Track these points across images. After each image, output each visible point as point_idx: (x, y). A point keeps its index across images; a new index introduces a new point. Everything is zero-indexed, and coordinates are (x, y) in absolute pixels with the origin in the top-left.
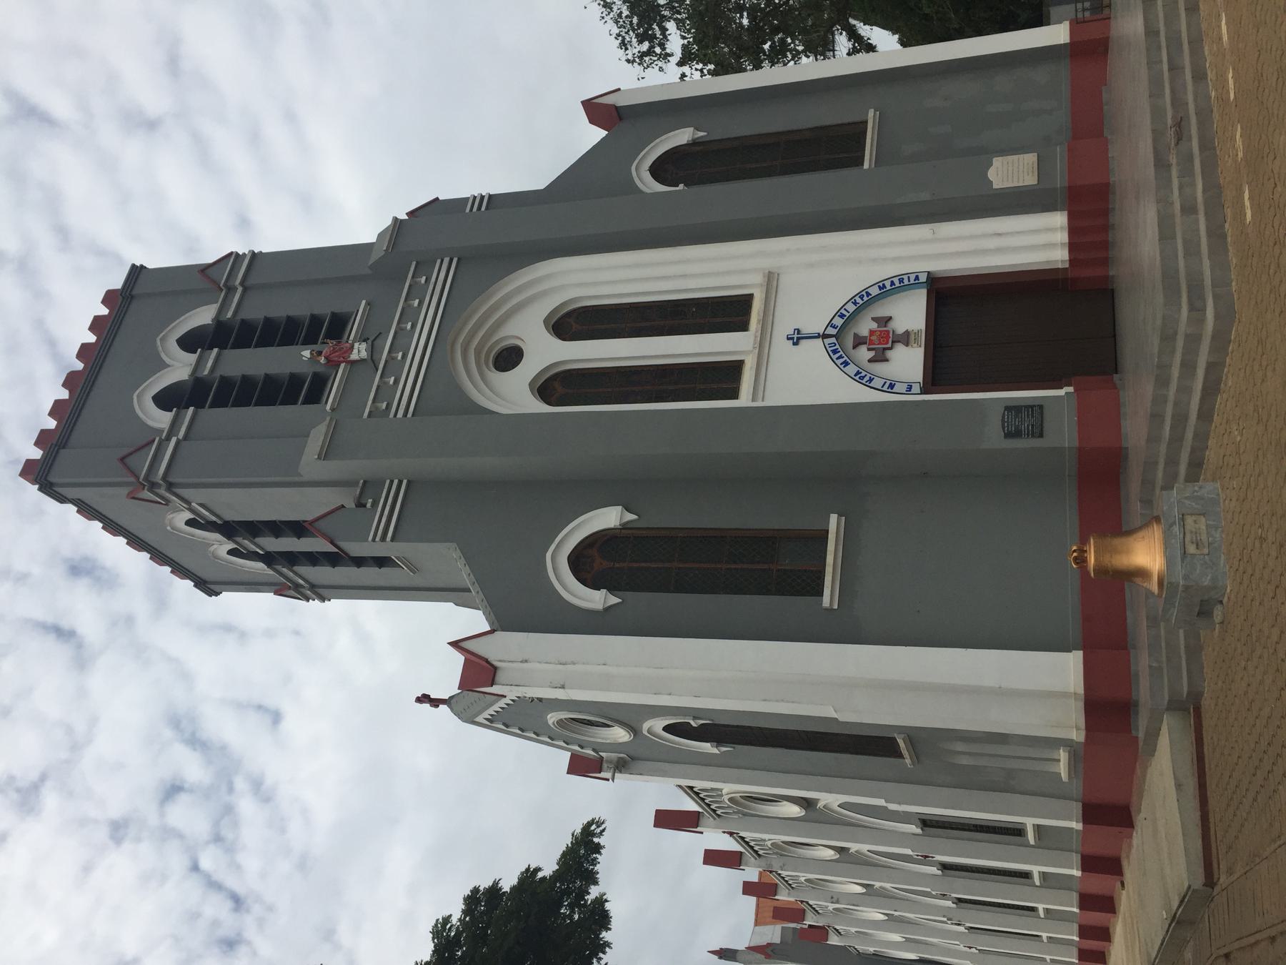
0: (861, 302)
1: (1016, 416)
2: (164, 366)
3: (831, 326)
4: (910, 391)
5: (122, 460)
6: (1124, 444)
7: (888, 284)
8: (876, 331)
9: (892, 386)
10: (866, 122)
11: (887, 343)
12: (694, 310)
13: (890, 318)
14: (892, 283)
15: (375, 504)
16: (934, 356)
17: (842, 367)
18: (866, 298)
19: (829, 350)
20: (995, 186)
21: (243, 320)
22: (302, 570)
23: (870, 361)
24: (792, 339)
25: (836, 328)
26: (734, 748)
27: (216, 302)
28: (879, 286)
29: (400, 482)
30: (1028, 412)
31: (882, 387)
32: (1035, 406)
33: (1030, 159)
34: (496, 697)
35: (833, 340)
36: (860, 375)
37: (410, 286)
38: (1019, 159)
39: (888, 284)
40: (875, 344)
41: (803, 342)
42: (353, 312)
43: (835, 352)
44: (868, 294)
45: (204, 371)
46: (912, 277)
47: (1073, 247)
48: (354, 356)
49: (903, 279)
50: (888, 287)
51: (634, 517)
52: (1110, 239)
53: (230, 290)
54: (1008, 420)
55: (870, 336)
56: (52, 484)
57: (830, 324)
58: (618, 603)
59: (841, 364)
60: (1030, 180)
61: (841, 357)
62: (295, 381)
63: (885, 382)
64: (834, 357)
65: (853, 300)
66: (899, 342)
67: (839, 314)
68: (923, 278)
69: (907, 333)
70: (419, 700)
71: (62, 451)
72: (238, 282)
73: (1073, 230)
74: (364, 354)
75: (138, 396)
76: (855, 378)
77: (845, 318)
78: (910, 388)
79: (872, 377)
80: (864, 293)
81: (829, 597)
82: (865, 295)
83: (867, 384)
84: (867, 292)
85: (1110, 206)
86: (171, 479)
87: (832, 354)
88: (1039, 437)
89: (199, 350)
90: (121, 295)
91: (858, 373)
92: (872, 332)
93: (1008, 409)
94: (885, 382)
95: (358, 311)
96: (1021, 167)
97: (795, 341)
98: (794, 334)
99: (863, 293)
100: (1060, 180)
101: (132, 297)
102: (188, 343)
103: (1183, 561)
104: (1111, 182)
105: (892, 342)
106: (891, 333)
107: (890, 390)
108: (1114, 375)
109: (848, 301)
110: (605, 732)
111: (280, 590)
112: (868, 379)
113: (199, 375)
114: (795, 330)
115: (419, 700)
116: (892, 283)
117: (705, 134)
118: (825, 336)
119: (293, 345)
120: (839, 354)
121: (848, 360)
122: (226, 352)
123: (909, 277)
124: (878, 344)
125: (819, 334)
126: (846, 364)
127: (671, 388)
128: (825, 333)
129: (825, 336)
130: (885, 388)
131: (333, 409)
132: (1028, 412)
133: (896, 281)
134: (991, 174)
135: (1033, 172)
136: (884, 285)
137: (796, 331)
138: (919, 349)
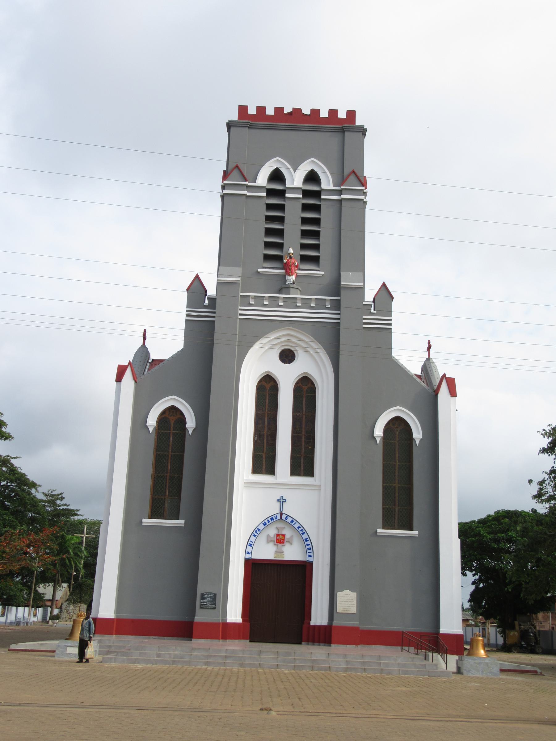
0: (299, 530)
1: (211, 598)
3: (287, 517)
4: (247, 553)
5: (237, 166)
6: (193, 639)
7: (309, 542)
8: (284, 537)
9: (250, 545)
10: (413, 530)
11: (277, 542)
12: (310, 448)
13: (291, 544)
14: (308, 545)
15: (206, 307)
16: (268, 564)
17: (263, 522)
18: (301, 532)
19: (274, 516)
20: (339, 593)
23: (268, 536)
24: (281, 499)
25: (285, 519)
27: (334, 186)
28: (307, 538)
29: (214, 317)
30: (212, 603)
31: (250, 541)
32: (215, 606)
33: (353, 609)
35: (279, 517)
36: (258, 531)
37: (325, 299)
38: (354, 604)
39: (309, 542)
40: (277, 537)
41: (279, 503)
42: (319, 267)
43: (272, 519)
44: (303, 533)
45: (288, 193)
46: (311, 554)
47: (314, 626)
48: (288, 277)
49: (310, 550)
50: (306, 543)
51: (190, 434)
52: (315, 643)
53: (340, 192)
54: (210, 595)
55: (281, 535)
57: (288, 516)
58: (150, 432)
59: (265, 522)
60: (340, 608)
61: (269, 521)
62: (280, 246)
63: (253, 542)
64: (269, 519)
65: (301, 526)
66: (278, 548)
67: (293, 520)
68: (310, 559)
69: (283, 552)
71: (247, 128)
72: (343, 196)
73: (320, 627)
74: (287, 283)
75: (278, 160)
76: (257, 528)
77: (291, 523)
78: (249, 553)
79: (256, 537)
80: (304, 531)
81: (146, 521)
82: (303, 532)
83: (253, 534)
84: (304, 533)
85: (326, 644)
87: (270, 517)
88: (201, 607)
90: (343, 127)
91: (259, 530)
92: (284, 535)
93: (215, 595)
94: (253, 542)
95: (318, 271)
96: (348, 605)
97: (279, 500)
98: (283, 499)
99: (304, 530)
100: (335, 623)
101: (344, 132)
102: (312, 177)
103: (65, 646)
104: (332, 645)
105: (278, 545)
106: (283, 544)
107: (248, 544)
108: (248, 641)
109: (300, 524)
112: (255, 535)
114: (286, 500)
116: (308, 545)
117: (417, 445)
118: (281, 514)
120: (270, 520)
121: (267, 525)
123: (311, 552)
124: (277, 539)
125: (282, 511)
126: (265, 524)
127: (265, 441)
128: (283, 515)
129: (281, 514)
130: (249, 542)
131: (258, 272)
132: (212, 603)
133: (310, 546)
134: (347, 592)
135: (345, 611)
136: (308, 540)
137: (285, 500)
138: (273, 557)
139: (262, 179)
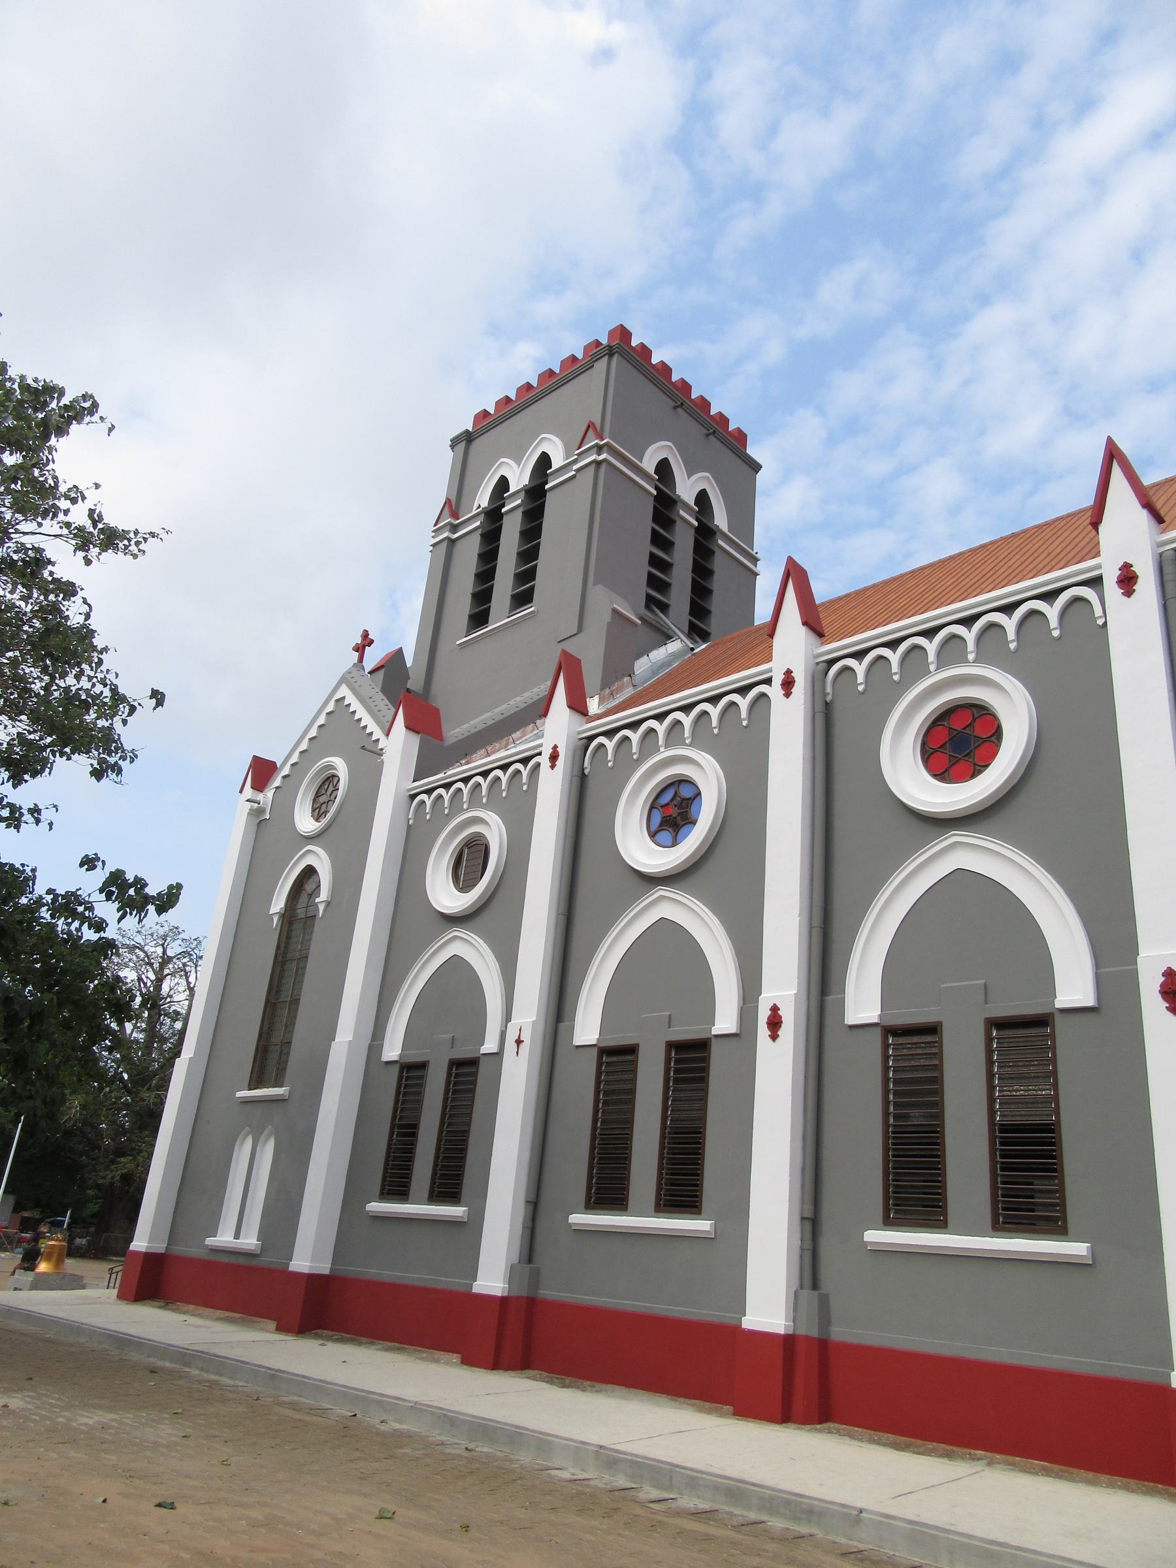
2: (690, 474)
21: (713, 552)
22: (476, 539)
26: (276, 928)
34: (388, 725)
56: (611, 355)
70: (366, 634)
75: (670, 447)
86: (604, 465)
89: (697, 509)
110: (307, 806)
111: (450, 506)
113: (679, 505)
115: (366, 634)
119: (692, 592)
122: (693, 531)
139: (649, 464)
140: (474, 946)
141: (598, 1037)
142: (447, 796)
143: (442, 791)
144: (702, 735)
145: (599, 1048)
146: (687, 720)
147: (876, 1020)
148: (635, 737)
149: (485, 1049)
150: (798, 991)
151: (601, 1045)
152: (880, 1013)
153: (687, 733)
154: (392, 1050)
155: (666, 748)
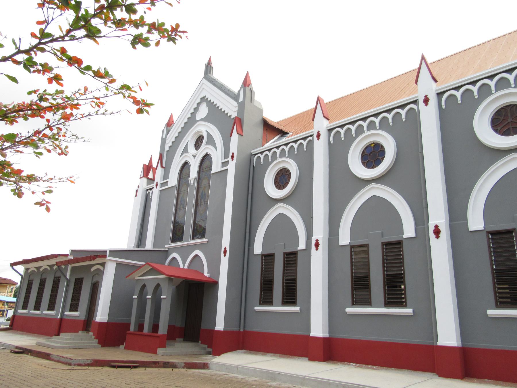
140: (289, 210)
141: (350, 241)
142: (270, 154)
143: (275, 150)
144: (384, 125)
145: (350, 246)
146: (377, 121)
147: (483, 229)
148: (353, 128)
149: (299, 249)
150: (445, 220)
151: (352, 245)
152: (484, 226)
153: (377, 125)
154: (258, 249)
155: (367, 131)
